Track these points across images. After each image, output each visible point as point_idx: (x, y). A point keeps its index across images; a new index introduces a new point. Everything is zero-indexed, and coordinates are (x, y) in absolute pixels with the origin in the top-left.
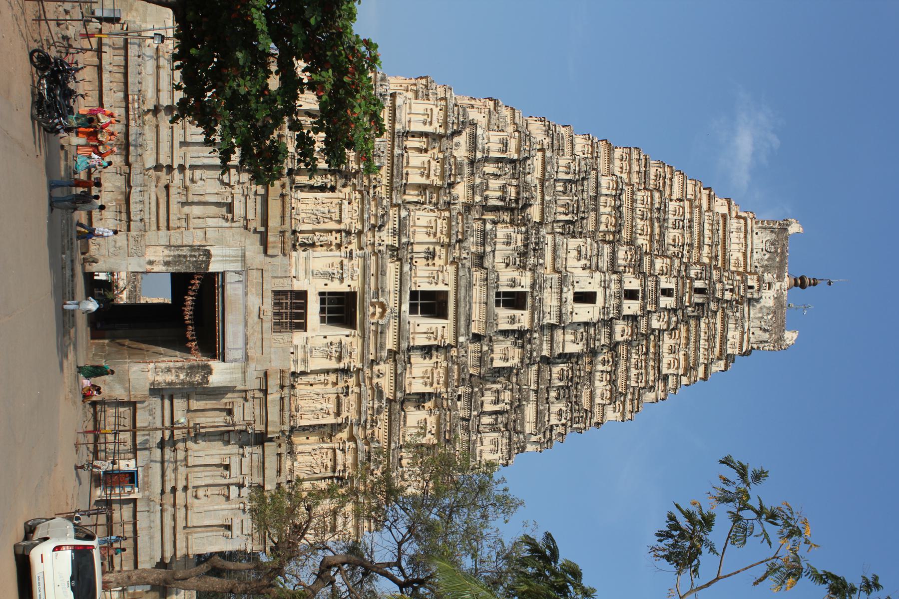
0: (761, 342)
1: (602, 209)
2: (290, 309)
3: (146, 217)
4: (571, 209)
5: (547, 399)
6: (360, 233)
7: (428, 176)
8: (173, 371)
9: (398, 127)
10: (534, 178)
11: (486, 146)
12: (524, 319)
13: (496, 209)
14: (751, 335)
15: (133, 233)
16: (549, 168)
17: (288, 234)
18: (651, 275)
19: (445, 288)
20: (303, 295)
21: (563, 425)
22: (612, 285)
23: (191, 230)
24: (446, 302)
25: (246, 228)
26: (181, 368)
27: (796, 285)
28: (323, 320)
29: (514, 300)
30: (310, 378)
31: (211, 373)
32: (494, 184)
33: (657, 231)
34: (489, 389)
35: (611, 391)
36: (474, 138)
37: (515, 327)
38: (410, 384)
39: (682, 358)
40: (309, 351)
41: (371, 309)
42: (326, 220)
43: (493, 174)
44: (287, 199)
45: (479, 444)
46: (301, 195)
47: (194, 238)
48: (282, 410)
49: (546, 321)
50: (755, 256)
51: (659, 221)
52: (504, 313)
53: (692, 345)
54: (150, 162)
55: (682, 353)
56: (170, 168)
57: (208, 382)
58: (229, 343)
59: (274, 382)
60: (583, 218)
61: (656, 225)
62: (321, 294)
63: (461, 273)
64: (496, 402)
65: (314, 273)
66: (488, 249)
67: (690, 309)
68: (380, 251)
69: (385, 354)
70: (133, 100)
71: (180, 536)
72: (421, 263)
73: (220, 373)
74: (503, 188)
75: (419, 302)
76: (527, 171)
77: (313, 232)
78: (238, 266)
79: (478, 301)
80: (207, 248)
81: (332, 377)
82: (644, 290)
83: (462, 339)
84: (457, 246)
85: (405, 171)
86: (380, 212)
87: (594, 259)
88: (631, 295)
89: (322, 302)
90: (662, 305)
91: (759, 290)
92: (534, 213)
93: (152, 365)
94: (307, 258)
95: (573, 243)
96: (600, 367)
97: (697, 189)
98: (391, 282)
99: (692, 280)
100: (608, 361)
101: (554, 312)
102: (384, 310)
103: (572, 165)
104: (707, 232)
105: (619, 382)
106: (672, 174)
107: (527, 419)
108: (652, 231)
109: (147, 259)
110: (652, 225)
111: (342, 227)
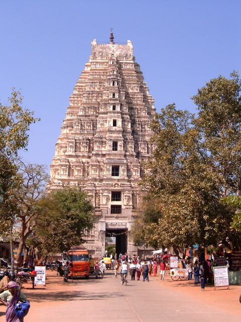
2: (116, 210)
15: (95, 249)
19: (111, 167)
20: (112, 206)
24: (115, 166)
40: (127, 205)
47: (96, 234)
51: (92, 94)
52: (119, 148)
61: (94, 95)
81: (134, 197)
88: (114, 108)
89: (114, 200)
95: (99, 126)
110: (94, 96)
111: (94, 195)
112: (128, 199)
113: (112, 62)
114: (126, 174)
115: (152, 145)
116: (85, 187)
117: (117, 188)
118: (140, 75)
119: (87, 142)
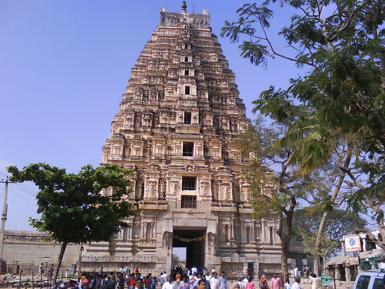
0: (206, 23)
1: (155, 83)
2: (188, 202)
3: (151, 256)
4: (154, 95)
5: (226, 105)
6: (160, 175)
7: (140, 148)
8: (210, 247)
9: (121, 159)
10: (142, 109)
11: (129, 126)
12: (194, 114)
13: (153, 123)
14: (204, 27)
15: (157, 261)
16: (138, 103)
17: (160, 201)
18: (179, 65)
19: (182, 143)
20: (183, 197)
21: (236, 100)
22: (183, 80)
23: (156, 239)
24: (188, 143)
25: (157, 218)
26: (209, 244)
27: (185, 10)
28: (193, 189)
29: (188, 118)
30: (215, 195)
31: (211, 233)
32: (144, 123)
33: (163, 63)
34: (221, 127)
35: (223, 81)
36: (126, 131)
38: (218, 157)
39: (211, 54)
40: (205, 195)
41: (189, 171)
42: (155, 187)
43: (140, 124)
44: (146, 201)
45: (242, 132)
46: (145, 196)
47: (160, 238)
48: (226, 206)
49: (196, 105)
51: (159, 62)
52: (192, 121)
53: (207, 50)
54: (130, 254)
55: (210, 54)
56: (132, 247)
57: (215, 234)
58: (200, 225)
59: (216, 209)
60: (158, 90)
62: (183, 190)
63: (177, 137)
64: (226, 125)
65: (175, 192)
66: (168, 126)
67: (193, 50)
68: (167, 167)
69: (206, 166)
70: (106, 260)
71: (274, 247)
72: (173, 152)
73: (212, 229)
74: (145, 120)
76: (139, 111)
77: (159, 192)
79: (187, 131)
80: (163, 233)
81: (215, 187)
82: (185, 68)
83: (202, 137)
84: (167, 138)
85: (138, 157)
86: (153, 167)
88: (187, 73)
89: (186, 189)
90: (191, 61)
91: (187, 24)
92: (155, 109)
93: (207, 255)
94: (169, 195)
95: (167, 94)
96: (214, 85)
97: (148, 47)
98: (180, 164)
99: (182, 49)
100: (212, 82)
101: (193, 102)
102: (190, 166)
103: (137, 94)
104: (165, 44)
105: (220, 78)
106: (141, 56)
107: (233, 113)
108: (163, 64)
109: (167, 256)
110: (161, 64)
111: (157, 181)
112: (206, 188)
113: (184, 26)
114: (203, 154)
115: (235, 121)
118: (218, 47)
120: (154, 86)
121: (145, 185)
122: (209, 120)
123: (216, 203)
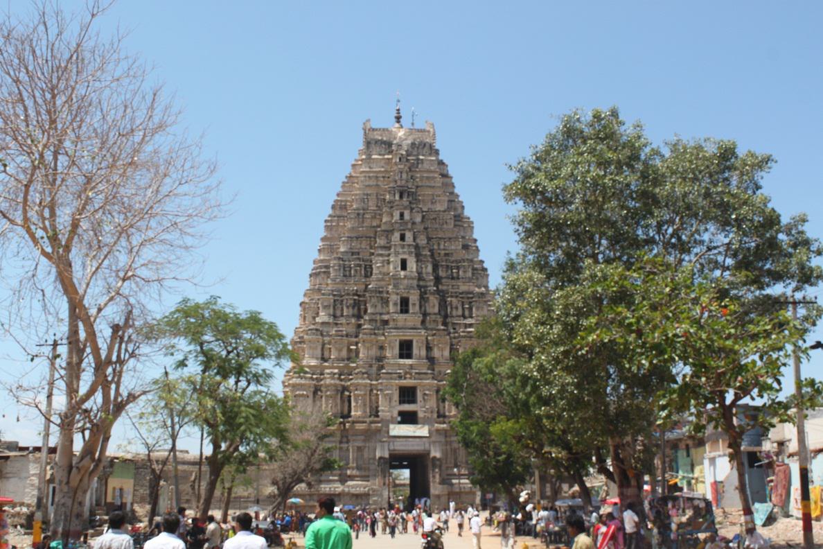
29: (404, 305)
36: (323, 323)
37: (418, 303)
46: (353, 413)
50: (383, 152)
58: (422, 448)
69: (429, 372)
74: (348, 307)
75: (405, 352)
77: (371, 407)
78: (386, 444)
87: (386, 258)
88: (403, 238)
93: (431, 484)
94: (383, 411)
96: (442, 247)
113: (398, 156)
115: (470, 303)
116: (352, 379)
117: (408, 382)
118: (446, 180)
119: (355, 300)
120: (358, 254)
121: (352, 399)
122: (433, 305)
123: (441, 419)
